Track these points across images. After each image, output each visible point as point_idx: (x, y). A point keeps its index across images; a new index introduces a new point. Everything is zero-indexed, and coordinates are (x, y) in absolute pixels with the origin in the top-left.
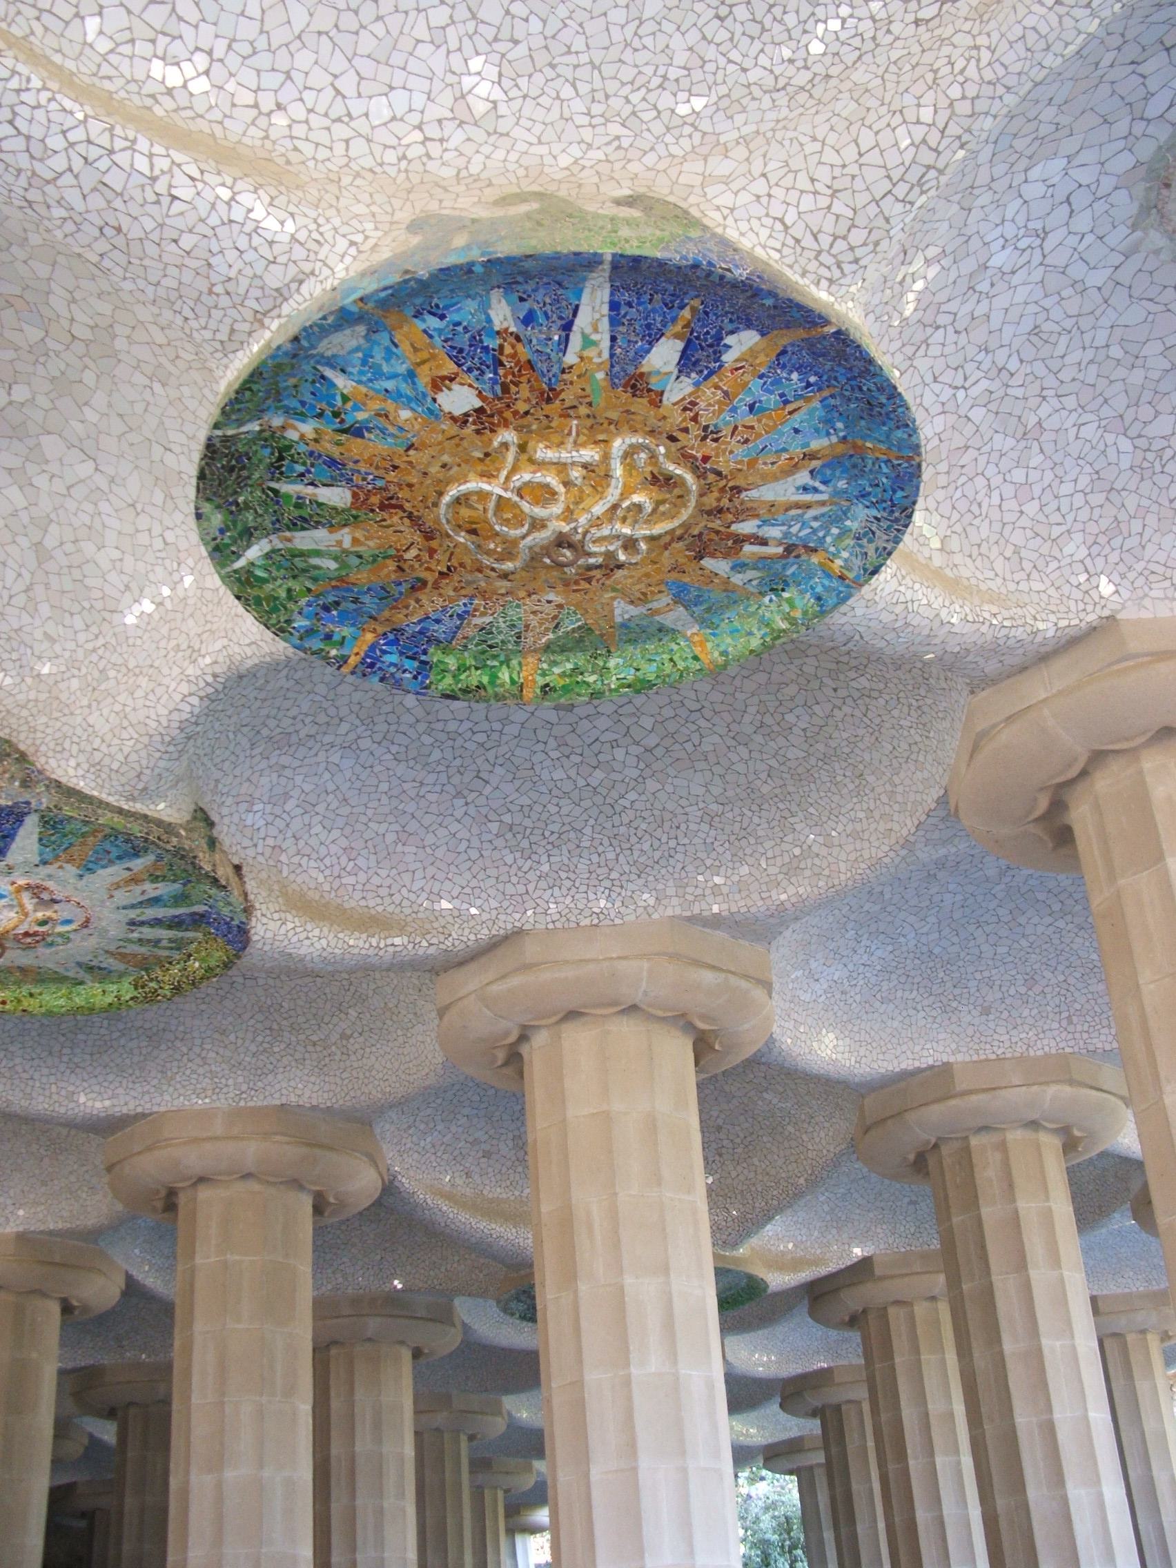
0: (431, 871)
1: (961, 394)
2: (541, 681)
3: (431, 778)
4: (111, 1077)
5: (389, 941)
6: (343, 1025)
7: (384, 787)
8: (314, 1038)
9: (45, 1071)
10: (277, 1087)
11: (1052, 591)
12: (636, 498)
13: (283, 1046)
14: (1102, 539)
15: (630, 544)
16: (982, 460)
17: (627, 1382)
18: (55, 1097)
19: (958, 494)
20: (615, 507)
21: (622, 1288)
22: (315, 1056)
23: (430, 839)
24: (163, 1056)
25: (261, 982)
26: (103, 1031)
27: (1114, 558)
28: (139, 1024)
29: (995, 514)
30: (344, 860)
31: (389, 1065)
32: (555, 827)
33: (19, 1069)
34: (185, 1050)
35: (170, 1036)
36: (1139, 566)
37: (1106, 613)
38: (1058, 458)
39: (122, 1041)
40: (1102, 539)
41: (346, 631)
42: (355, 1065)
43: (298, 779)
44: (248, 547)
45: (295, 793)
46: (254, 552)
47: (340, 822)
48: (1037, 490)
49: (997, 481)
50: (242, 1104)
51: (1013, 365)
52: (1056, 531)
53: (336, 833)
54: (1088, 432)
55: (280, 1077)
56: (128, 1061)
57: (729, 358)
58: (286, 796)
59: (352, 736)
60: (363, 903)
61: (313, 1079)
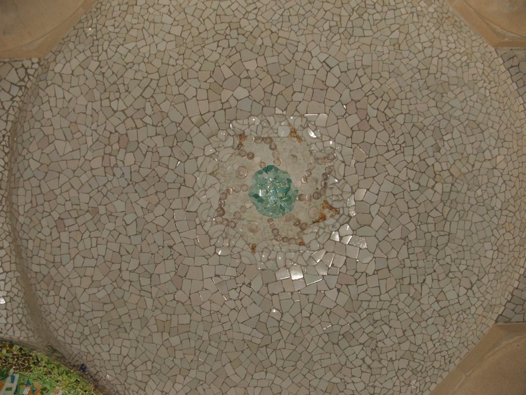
24: (452, 73)
26: (456, 134)
28: (435, 111)
34: (435, 61)
35: (431, 81)
56: (475, 98)
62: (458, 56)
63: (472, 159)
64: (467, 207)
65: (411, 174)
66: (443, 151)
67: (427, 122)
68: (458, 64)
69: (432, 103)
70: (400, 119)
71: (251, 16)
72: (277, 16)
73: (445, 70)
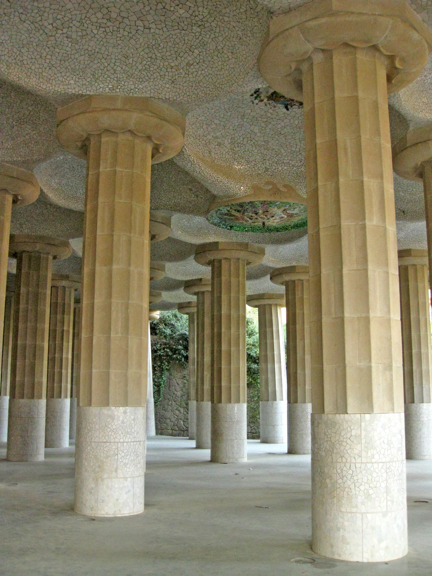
4: (68, 74)
6: (189, 58)
8: (173, 64)
9: (37, 66)
10: (149, 88)
13: (155, 67)
17: (364, 227)
18: (41, 80)
21: (362, 182)
22: (170, 74)
25: (152, 31)
26: (68, 49)
28: (86, 47)
31: (211, 80)
33: (25, 63)
34: (106, 64)
35: (100, 56)
39: (77, 56)
42: (191, 80)
50: (131, 95)
55: (151, 83)
61: (167, 86)
62: (100, 74)
63: (52, 49)
64: (31, 35)
65: (66, 19)
66: (66, 39)
67: (84, 41)
68: (97, 72)
69: (90, 49)
70: (95, 32)
71: (197, 34)
72: (186, 38)
73: (99, 65)
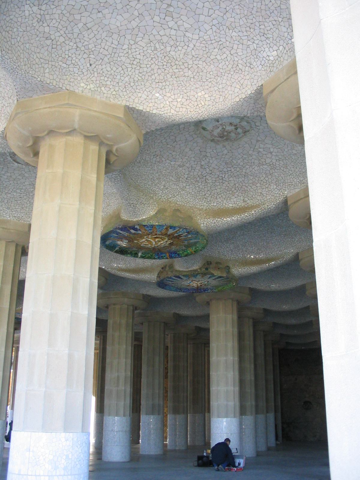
0: (277, 247)
1: (223, 179)
2: (193, 251)
3: (264, 233)
5: (271, 264)
7: (256, 237)
11: (272, 197)
12: (156, 240)
14: (277, 183)
15: (167, 242)
16: (241, 184)
18: (285, 286)
19: (241, 191)
20: (155, 242)
23: (273, 242)
27: (282, 185)
29: (252, 190)
30: (259, 251)
32: (293, 232)
36: (287, 184)
37: (285, 197)
38: (255, 175)
40: (277, 183)
41: (164, 255)
43: (238, 243)
44: (138, 255)
45: (240, 245)
46: (140, 254)
47: (253, 245)
48: (257, 182)
49: (247, 185)
51: (229, 169)
52: (267, 186)
53: (254, 247)
54: (256, 168)
57: (138, 228)
58: (238, 246)
59: (242, 233)
60: (266, 257)
